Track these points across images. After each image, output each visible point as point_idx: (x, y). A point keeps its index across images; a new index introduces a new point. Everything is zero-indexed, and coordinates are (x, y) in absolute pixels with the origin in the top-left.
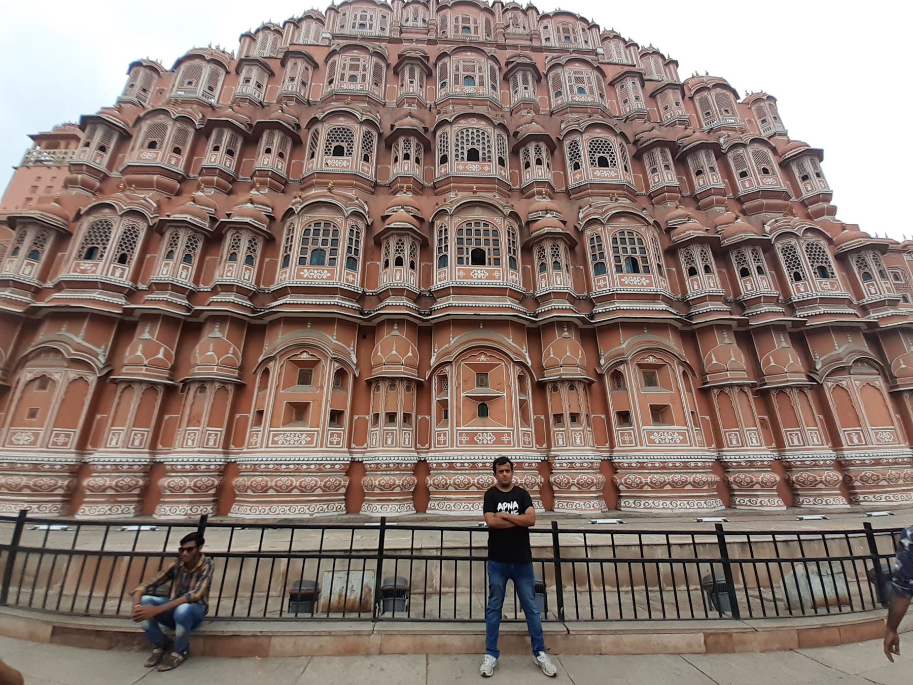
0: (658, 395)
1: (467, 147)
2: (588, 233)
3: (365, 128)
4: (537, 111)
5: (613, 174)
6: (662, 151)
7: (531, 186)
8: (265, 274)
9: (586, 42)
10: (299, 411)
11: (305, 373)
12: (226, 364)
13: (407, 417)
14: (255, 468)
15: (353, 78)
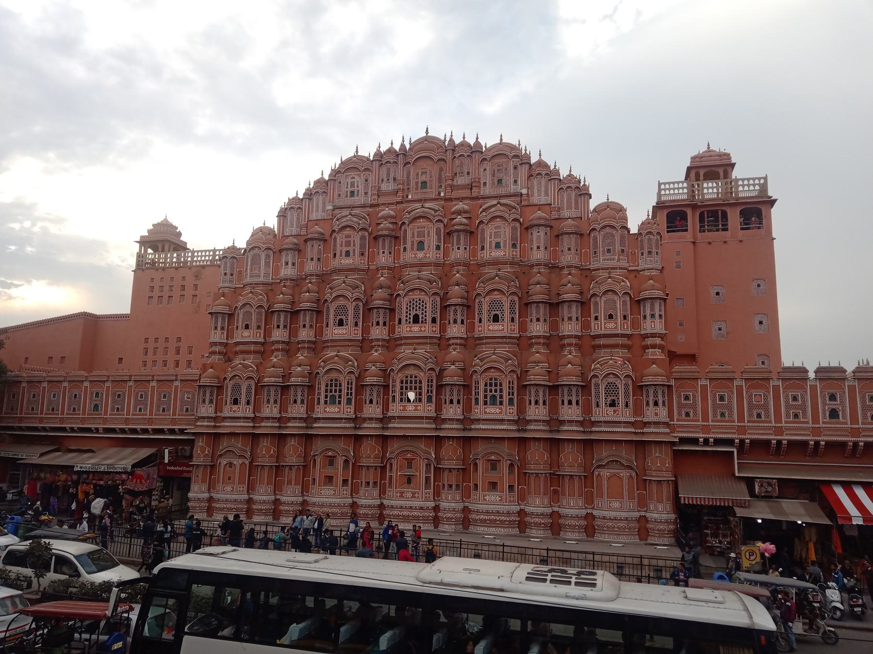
0: (493, 476)
1: (413, 313)
2: (474, 377)
3: (354, 304)
4: (465, 265)
5: (501, 327)
6: (538, 306)
7: (449, 339)
8: (310, 408)
9: (515, 181)
10: (329, 479)
11: (331, 461)
12: (299, 456)
13: (375, 483)
14: (314, 504)
15: (348, 254)
